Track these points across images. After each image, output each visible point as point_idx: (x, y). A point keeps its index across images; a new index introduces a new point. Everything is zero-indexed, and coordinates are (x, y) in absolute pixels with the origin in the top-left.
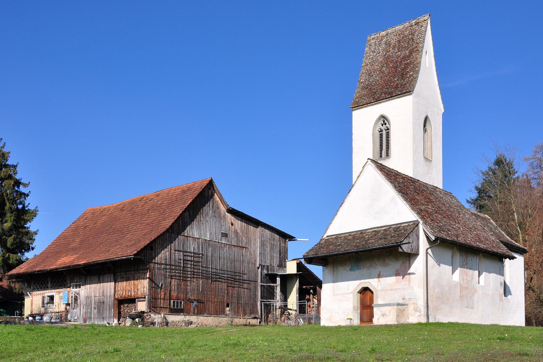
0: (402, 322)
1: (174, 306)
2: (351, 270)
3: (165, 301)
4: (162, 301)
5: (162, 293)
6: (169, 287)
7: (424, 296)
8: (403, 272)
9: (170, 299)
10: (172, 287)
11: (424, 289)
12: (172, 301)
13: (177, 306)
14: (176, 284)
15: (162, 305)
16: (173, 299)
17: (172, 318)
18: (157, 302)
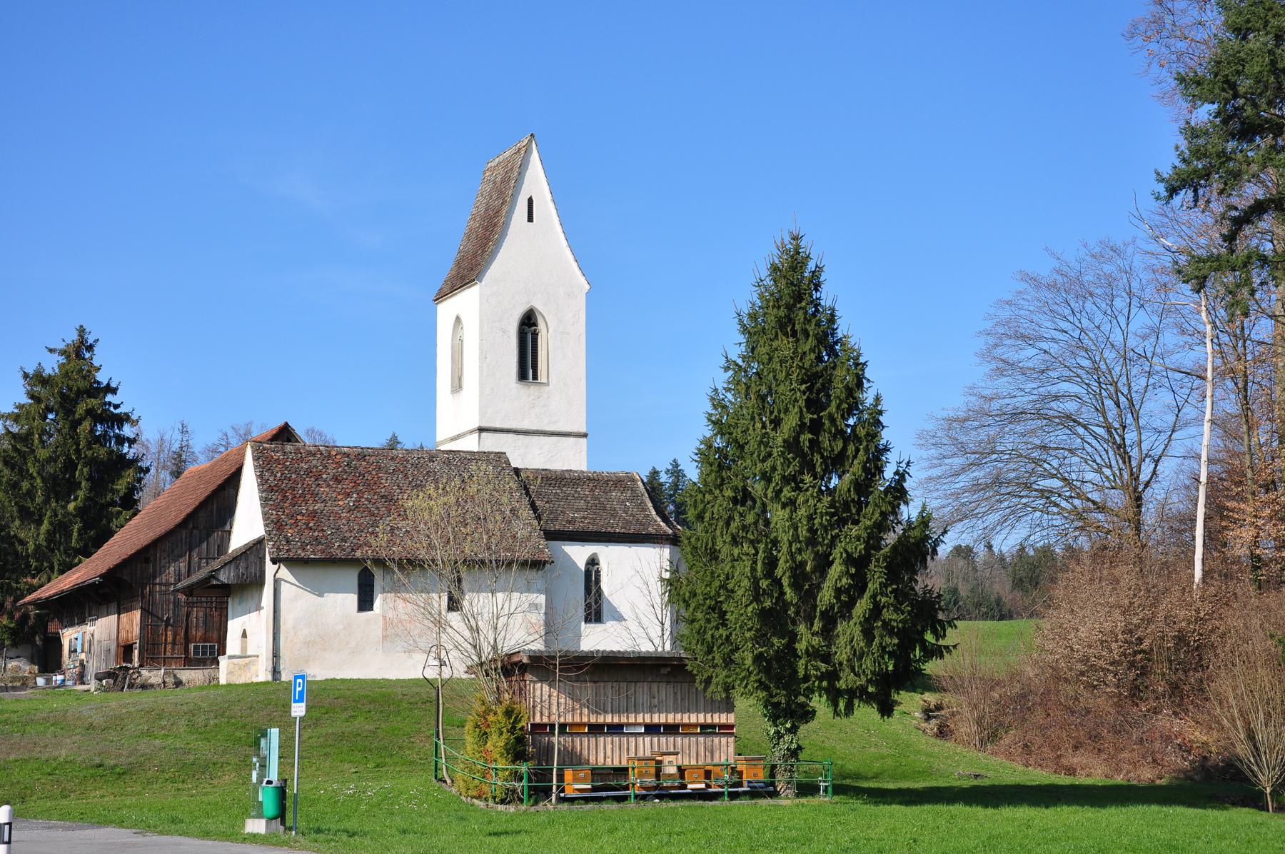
0: (242, 680)
1: (196, 653)
2: (239, 604)
3: (176, 647)
4: (169, 647)
5: (169, 633)
6: (185, 623)
7: (267, 642)
8: (259, 608)
9: (187, 640)
10: (192, 621)
11: (267, 633)
12: (192, 646)
13: (204, 653)
14: (201, 614)
15: (169, 654)
16: (196, 642)
17: (186, 675)
18: (158, 648)
